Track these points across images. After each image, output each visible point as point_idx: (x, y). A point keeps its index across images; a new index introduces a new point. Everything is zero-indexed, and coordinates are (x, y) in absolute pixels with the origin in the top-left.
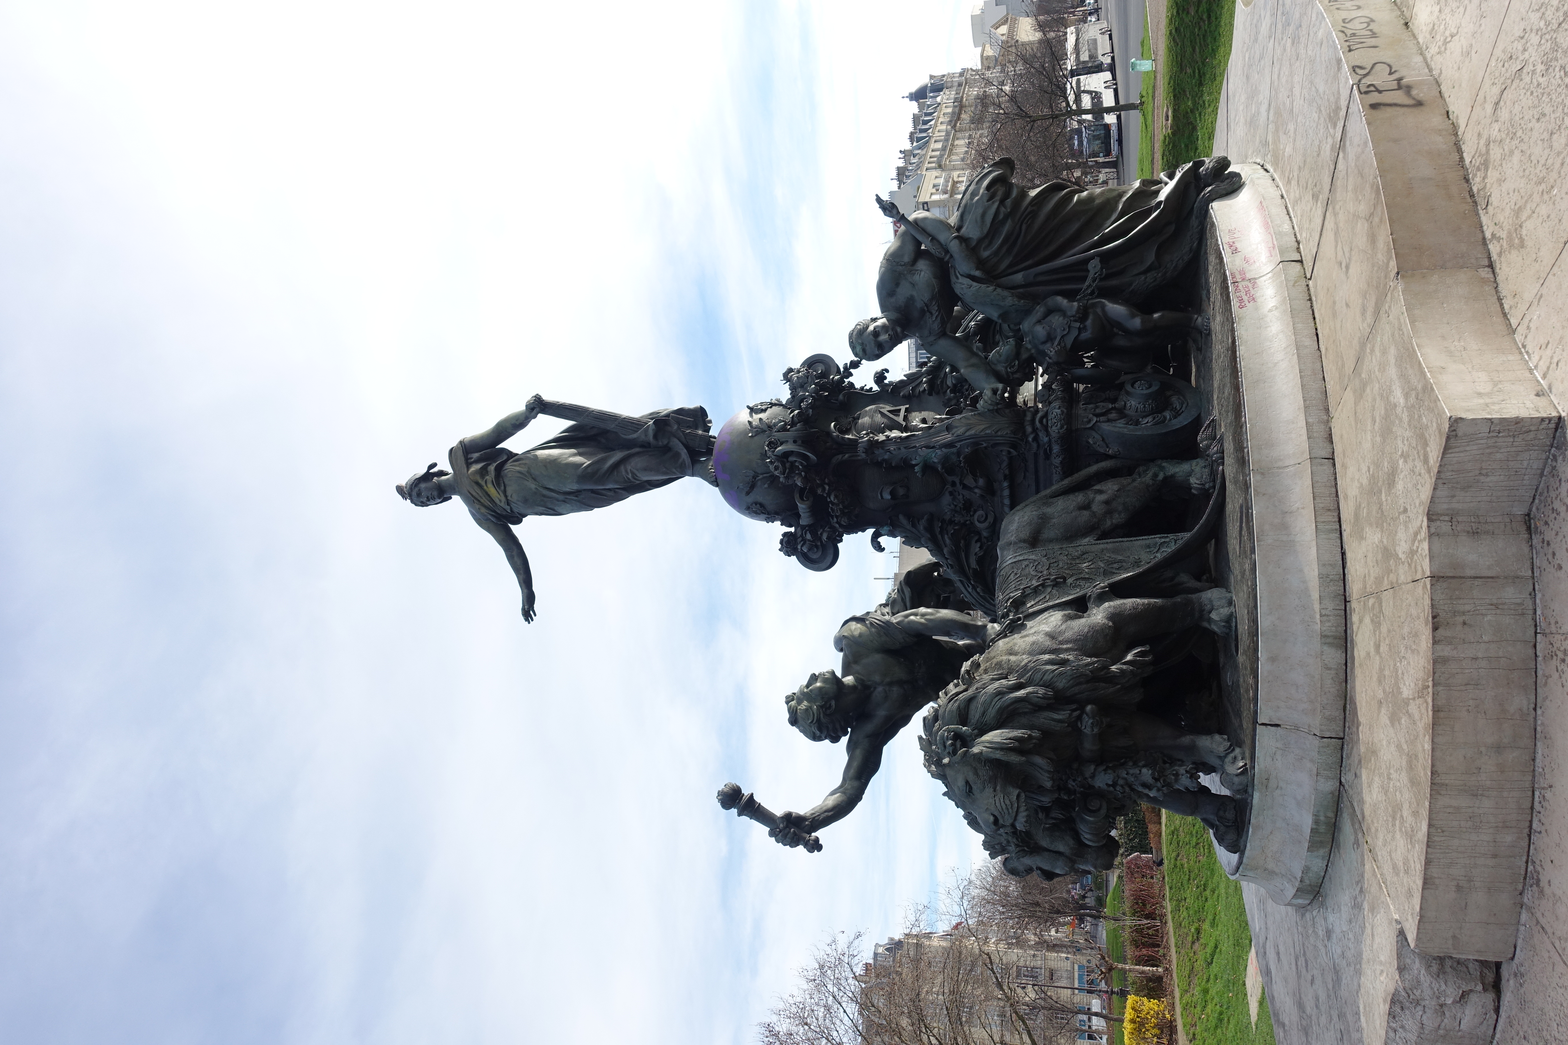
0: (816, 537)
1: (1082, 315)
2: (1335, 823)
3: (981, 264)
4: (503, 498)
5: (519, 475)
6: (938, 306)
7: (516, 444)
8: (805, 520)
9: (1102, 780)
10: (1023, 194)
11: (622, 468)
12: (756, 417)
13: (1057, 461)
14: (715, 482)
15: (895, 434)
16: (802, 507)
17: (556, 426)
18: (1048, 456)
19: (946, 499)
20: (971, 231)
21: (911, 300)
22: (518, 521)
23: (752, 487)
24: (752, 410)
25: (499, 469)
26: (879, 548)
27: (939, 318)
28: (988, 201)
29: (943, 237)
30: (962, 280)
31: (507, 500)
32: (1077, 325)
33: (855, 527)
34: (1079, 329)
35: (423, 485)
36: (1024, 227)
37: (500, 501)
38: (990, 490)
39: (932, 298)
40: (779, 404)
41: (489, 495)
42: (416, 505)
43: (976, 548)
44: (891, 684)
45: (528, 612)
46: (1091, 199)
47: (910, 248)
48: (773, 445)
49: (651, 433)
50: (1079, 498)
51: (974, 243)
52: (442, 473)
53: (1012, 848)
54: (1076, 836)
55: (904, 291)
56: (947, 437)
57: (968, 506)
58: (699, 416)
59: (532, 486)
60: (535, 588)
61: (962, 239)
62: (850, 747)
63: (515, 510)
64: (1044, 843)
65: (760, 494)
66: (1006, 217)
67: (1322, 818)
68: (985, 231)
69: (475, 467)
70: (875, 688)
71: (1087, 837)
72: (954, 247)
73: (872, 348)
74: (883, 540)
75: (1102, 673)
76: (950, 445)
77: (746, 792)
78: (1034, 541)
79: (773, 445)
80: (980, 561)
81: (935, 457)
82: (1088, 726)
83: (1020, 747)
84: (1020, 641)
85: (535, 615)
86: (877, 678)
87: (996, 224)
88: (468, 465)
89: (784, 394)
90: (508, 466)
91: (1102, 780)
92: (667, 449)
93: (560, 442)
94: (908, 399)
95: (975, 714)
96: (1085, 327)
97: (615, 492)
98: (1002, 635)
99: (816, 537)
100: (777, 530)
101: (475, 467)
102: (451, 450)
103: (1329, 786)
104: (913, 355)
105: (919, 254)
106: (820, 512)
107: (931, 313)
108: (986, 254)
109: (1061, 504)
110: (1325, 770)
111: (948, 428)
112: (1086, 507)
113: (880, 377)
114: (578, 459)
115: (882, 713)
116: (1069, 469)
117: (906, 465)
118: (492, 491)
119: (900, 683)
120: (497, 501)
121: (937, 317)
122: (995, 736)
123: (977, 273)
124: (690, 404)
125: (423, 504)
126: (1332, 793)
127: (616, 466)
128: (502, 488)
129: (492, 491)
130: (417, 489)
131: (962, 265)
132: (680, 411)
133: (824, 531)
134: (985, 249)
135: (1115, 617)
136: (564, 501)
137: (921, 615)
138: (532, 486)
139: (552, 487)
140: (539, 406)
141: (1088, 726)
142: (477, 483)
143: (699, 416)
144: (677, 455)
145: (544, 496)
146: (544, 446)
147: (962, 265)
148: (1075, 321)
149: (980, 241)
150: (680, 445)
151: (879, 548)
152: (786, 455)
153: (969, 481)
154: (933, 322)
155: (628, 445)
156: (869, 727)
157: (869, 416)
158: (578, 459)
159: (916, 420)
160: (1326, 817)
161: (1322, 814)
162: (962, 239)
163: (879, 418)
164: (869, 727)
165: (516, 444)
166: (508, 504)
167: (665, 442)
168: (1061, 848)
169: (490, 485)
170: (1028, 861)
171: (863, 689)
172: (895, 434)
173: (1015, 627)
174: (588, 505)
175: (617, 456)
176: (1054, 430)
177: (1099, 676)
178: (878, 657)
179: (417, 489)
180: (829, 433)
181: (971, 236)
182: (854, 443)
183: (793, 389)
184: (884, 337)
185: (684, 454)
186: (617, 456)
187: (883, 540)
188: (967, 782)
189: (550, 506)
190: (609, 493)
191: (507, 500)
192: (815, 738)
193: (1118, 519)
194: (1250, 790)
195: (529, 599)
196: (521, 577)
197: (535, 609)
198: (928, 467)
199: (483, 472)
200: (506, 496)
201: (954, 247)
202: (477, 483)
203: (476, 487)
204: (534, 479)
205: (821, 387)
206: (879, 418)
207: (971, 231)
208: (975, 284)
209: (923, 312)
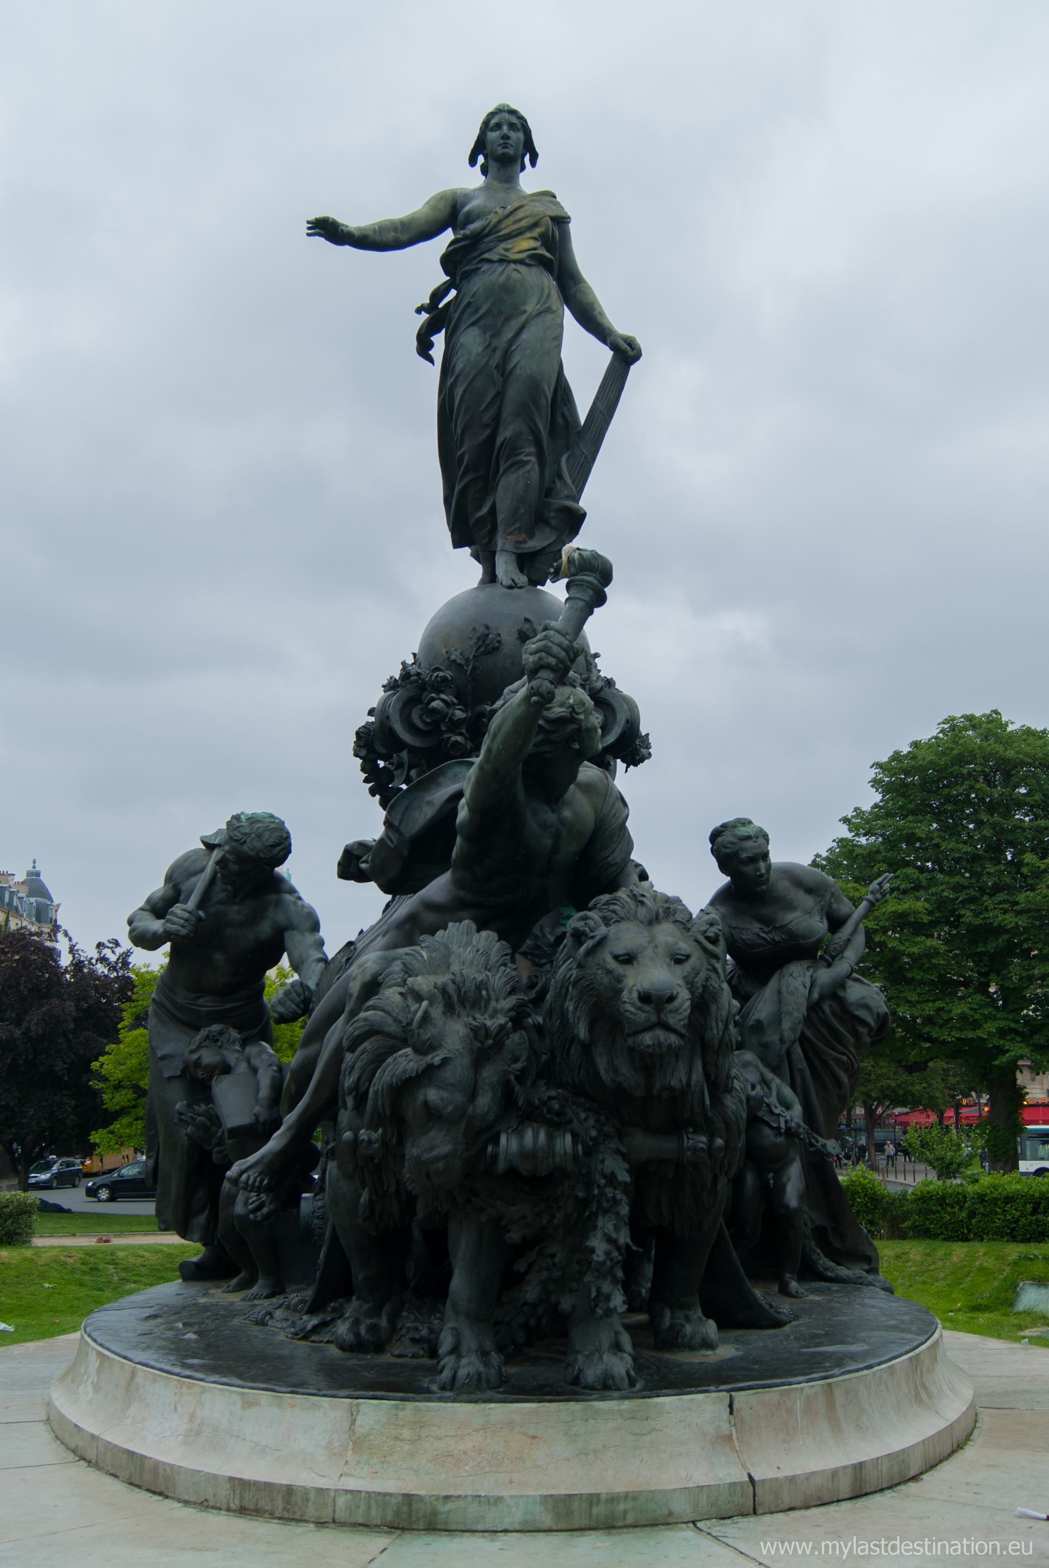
2: (613, 1527)
4: (512, 256)
5: (546, 292)
6: (779, 942)
11: (532, 449)
27: (761, 942)
28: (878, 1014)
30: (809, 973)
31: (509, 262)
32: (783, 1126)
34: (779, 1128)
35: (521, 135)
36: (845, 1058)
37: (507, 250)
39: (792, 935)
41: (516, 236)
42: (492, 115)
44: (557, 837)
49: (570, 503)
51: (841, 993)
52: (523, 168)
60: (347, 248)
63: (485, 267)
66: (856, 1035)
67: (622, 1506)
68: (852, 1008)
70: (553, 811)
75: (726, 1163)
85: (308, 235)
86: (567, 813)
96: (780, 1134)
97: (487, 426)
102: (554, 197)
103: (680, 1506)
107: (769, 932)
108: (826, 1007)
110: (708, 1497)
119: (555, 849)
120: (504, 245)
121: (763, 938)
123: (816, 995)
126: (671, 1514)
128: (528, 261)
130: (519, 126)
133: (466, 739)
134: (830, 1006)
136: (489, 346)
139: (524, 336)
142: (536, 225)
145: (508, 319)
148: (786, 1122)
149: (841, 1002)
150: (546, 543)
160: (625, 1512)
161: (630, 1505)
166: (501, 261)
167: (553, 522)
169: (532, 244)
179: (519, 126)
181: (848, 990)
185: (533, 544)
188: (688, 957)
189: (482, 322)
190: (487, 418)
191: (509, 262)
194: (616, 1394)
196: (371, 233)
197: (317, 238)
200: (515, 262)
202: (536, 225)
203: (531, 221)
204: (539, 314)
208: (807, 991)
209: (767, 922)
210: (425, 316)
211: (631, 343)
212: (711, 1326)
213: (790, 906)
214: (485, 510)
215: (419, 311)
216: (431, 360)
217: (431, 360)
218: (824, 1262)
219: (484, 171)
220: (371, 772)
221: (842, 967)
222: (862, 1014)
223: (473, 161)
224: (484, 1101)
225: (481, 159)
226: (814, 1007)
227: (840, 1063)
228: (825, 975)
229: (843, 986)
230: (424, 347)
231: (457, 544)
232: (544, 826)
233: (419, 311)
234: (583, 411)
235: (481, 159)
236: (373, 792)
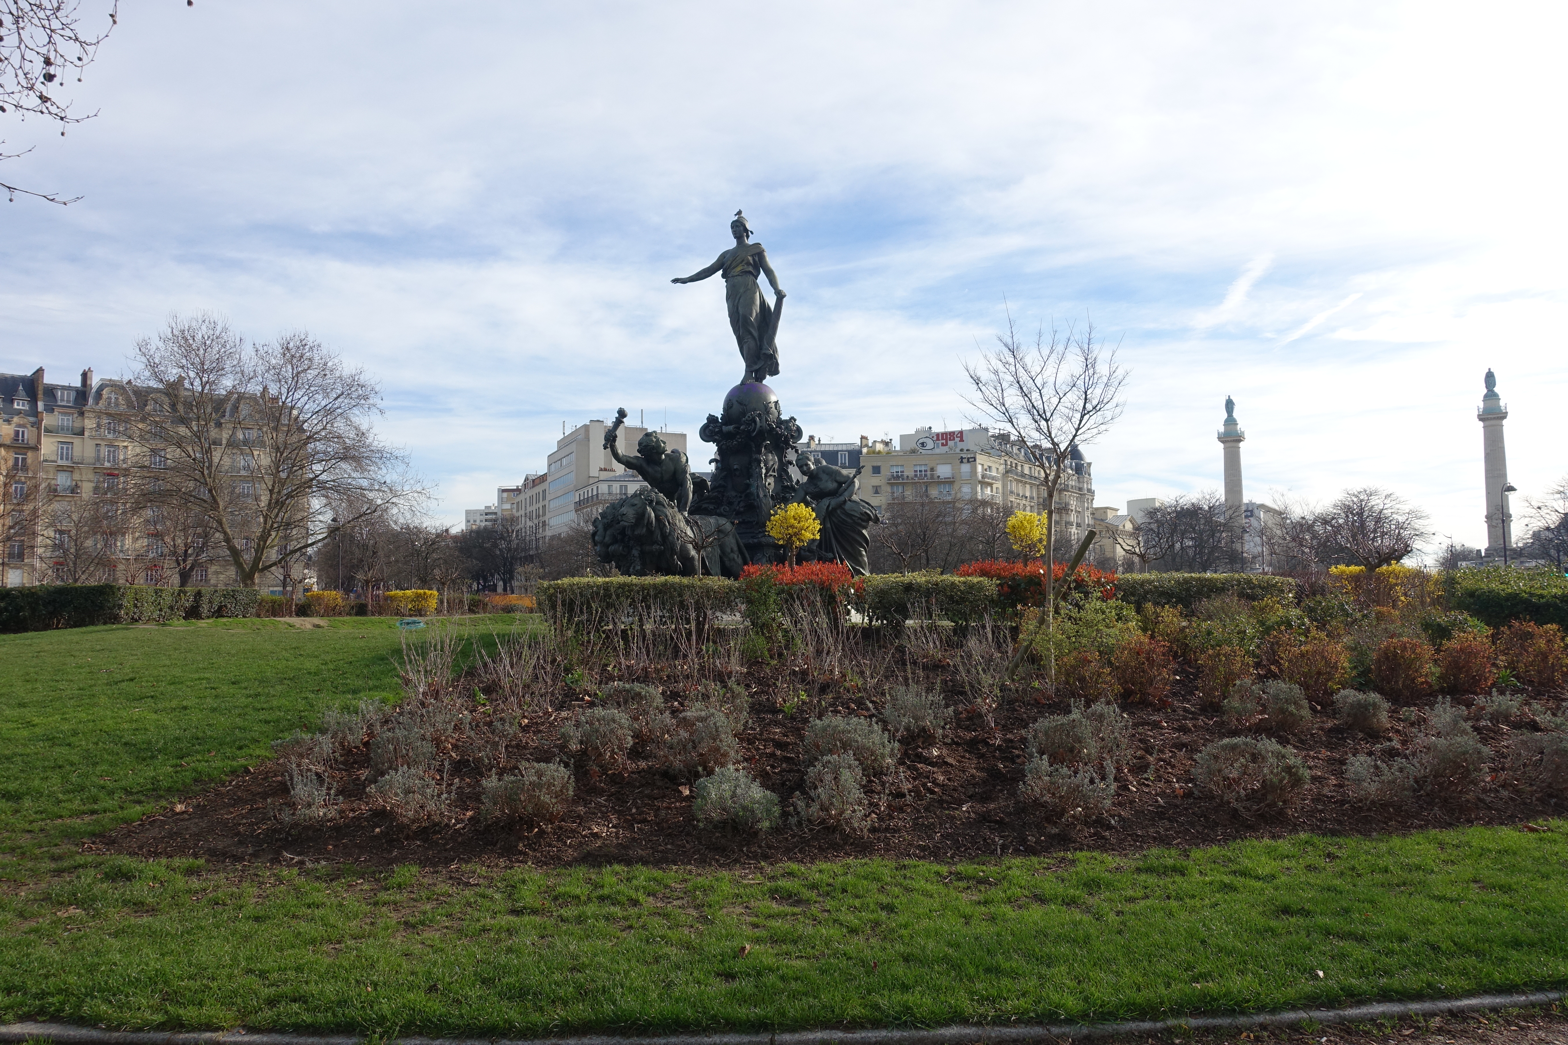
0: (716, 433)
3: (834, 509)
7: (762, 279)
8: (725, 428)
9: (635, 552)
10: (865, 528)
12: (773, 405)
13: (751, 541)
14: (743, 383)
15: (764, 471)
16: (731, 428)
17: (771, 301)
18: (753, 537)
19: (734, 494)
20: (848, 505)
21: (821, 480)
22: (723, 276)
23: (740, 403)
24: (776, 403)
25: (750, 272)
26: (710, 462)
29: (846, 494)
33: (720, 451)
38: (738, 513)
40: (779, 414)
43: (711, 507)
45: (676, 281)
46: (862, 555)
47: (842, 480)
48: (759, 415)
50: (735, 548)
52: (748, 237)
53: (605, 521)
54: (612, 544)
55: (824, 477)
56: (761, 495)
57: (730, 504)
58: (775, 371)
59: (742, 290)
61: (845, 501)
62: (637, 457)
64: (608, 533)
65: (736, 408)
69: (750, 258)
71: (611, 548)
72: (842, 498)
73: (801, 463)
74: (713, 464)
76: (758, 496)
77: (625, 420)
78: (720, 531)
79: (759, 415)
80: (706, 509)
81: (753, 489)
82: (656, 547)
83: (650, 523)
84: (682, 524)
87: (851, 516)
88: (752, 256)
89: (784, 417)
90: (752, 277)
91: (635, 552)
92: (759, 358)
93: (763, 303)
94: (780, 476)
95: (659, 507)
98: (685, 518)
99: (716, 433)
100: (718, 413)
101: (750, 258)
104: (844, 448)
105: (840, 484)
106: (729, 436)
109: (733, 541)
111: (765, 496)
112: (732, 551)
113: (790, 463)
114: (754, 314)
115: (650, 470)
116: (747, 546)
117: (750, 476)
118: (739, 268)
122: (653, 515)
124: (780, 368)
125: (732, 227)
127: (751, 334)
129: (739, 268)
131: (834, 502)
132: (777, 364)
135: (693, 557)
137: (690, 486)
138: (742, 290)
140: (780, 296)
141: (656, 547)
143: (775, 371)
144: (756, 364)
146: (761, 296)
147: (834, 502)
151: (710, 462)
152: (755, 422)
153: (742, 504)
154: (811, 489)
155: (761, 338)
156: (644, 465)
157: (773, 459)
158: (754, 314)
159: (771, 480)
162: (845, 501)
163: (771, 463)
164: (644, 465)
165: (762, 279)
168: (607, 539)
170: (600, 527)
171: (659, 462)
172: (764, 471)
173: (688, 522)
174: (730, 316)
175: (755, 334)
176: (763, 540)
177: (673, 551)
178: (672, 468)
180: (765, 440)
182: (760, 453)
183: (786, 421)
184: (805, 468)
185: (757, 367)
186: (755, 334)
187: (713, 464)
192: (640, 444)
193: (727, 563)
195: (684, 281)
198: (748, 486)
199: (748, 264)
201: (842, 498)
205: (786, 437)
206: (771, 463)
207: (848, 505)
224: (607, 539)
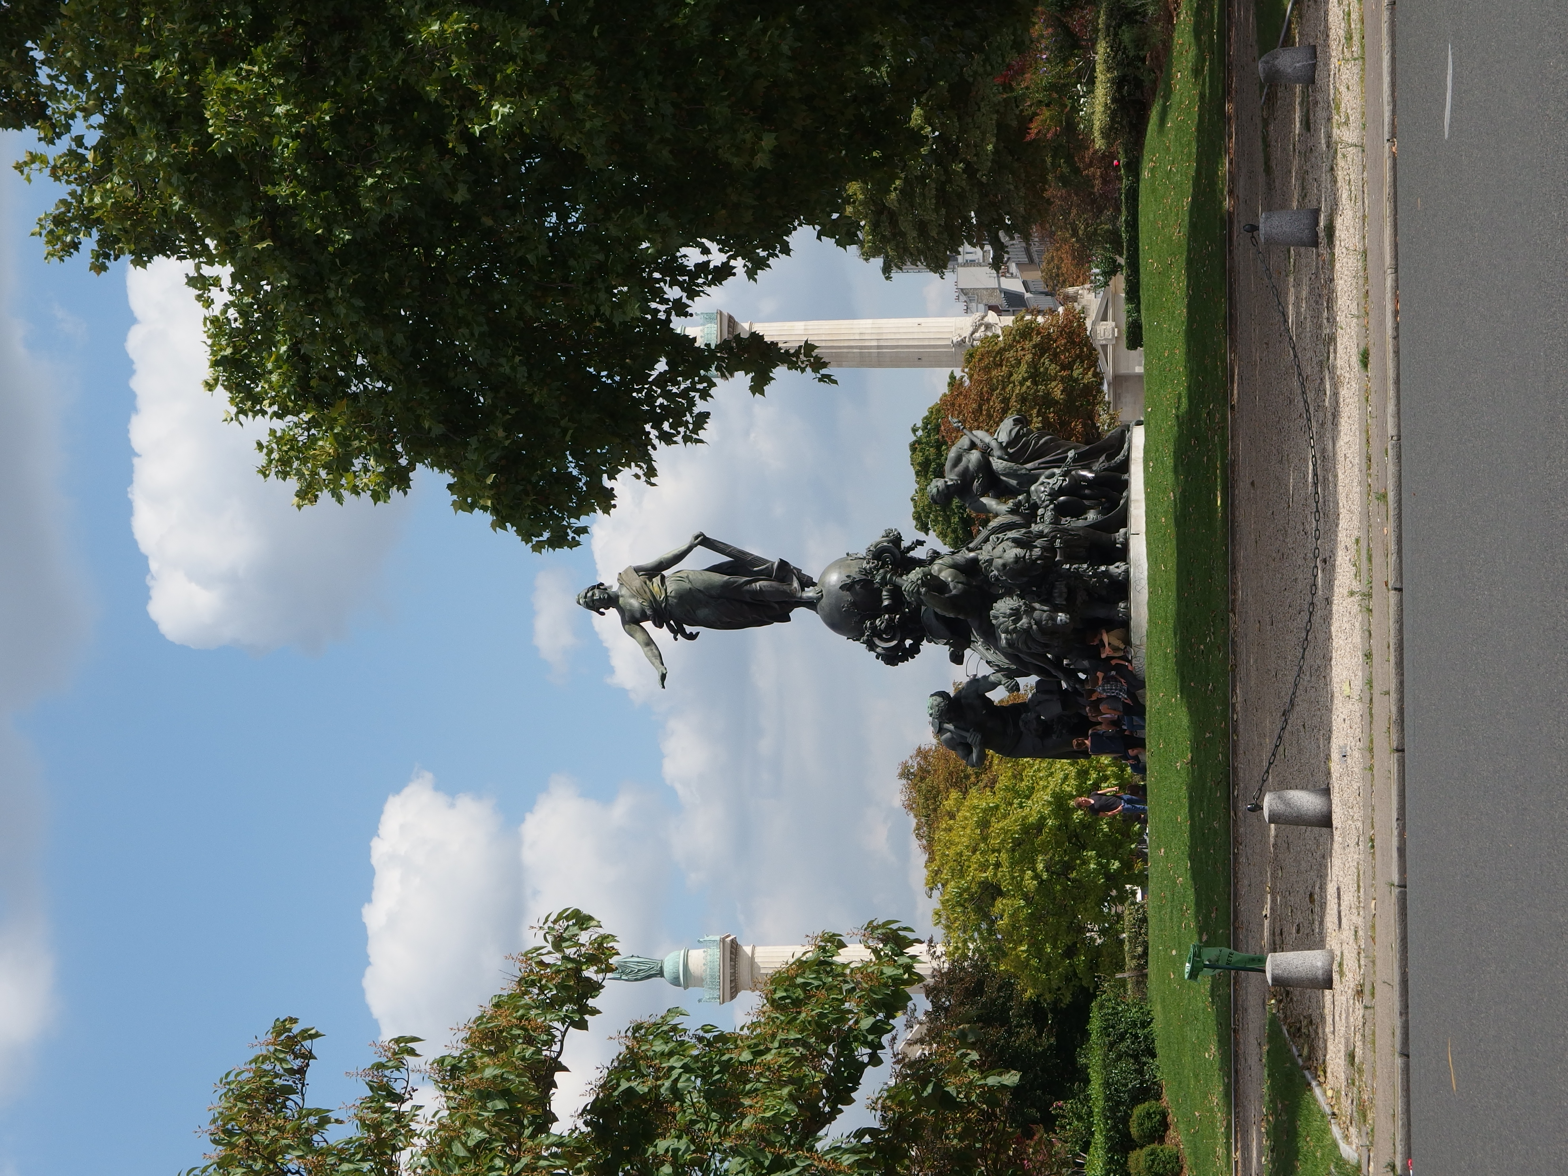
1: (1065, 474)
66: (1024, 435)
108: (1011, 451)
210: (679, 636)
211: (697, 538)
212: (1122, 531)
213: (967, 468)
214: (777, 606)
215: (676, 639)
216: (698, 633)
217: (698, 633)
218: (1120, 457)
219: (607, 608)
220: (904, 659)
221: (994, 444)
222: (1014, 433)
223: (603, 614)
225: (602, 610)
226: (1011, 458)
227: (1036, 443)
228: (997, 452)
229: (1001, 443)
230: (692, 637)
231: (788, 619)
232: (955, 588)
233: (676, 639)
234: (727, 559)
235: (602, 610)
236: (913, 657)
